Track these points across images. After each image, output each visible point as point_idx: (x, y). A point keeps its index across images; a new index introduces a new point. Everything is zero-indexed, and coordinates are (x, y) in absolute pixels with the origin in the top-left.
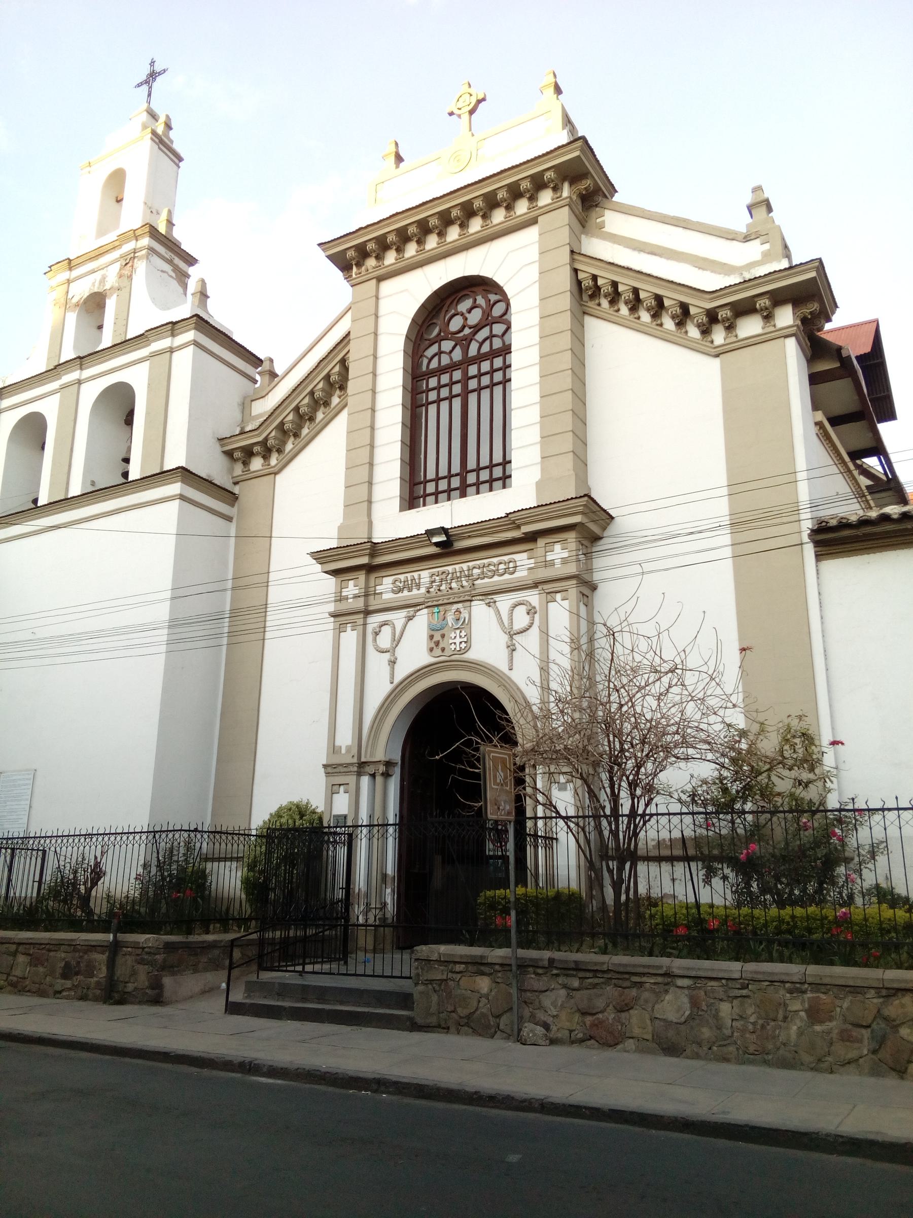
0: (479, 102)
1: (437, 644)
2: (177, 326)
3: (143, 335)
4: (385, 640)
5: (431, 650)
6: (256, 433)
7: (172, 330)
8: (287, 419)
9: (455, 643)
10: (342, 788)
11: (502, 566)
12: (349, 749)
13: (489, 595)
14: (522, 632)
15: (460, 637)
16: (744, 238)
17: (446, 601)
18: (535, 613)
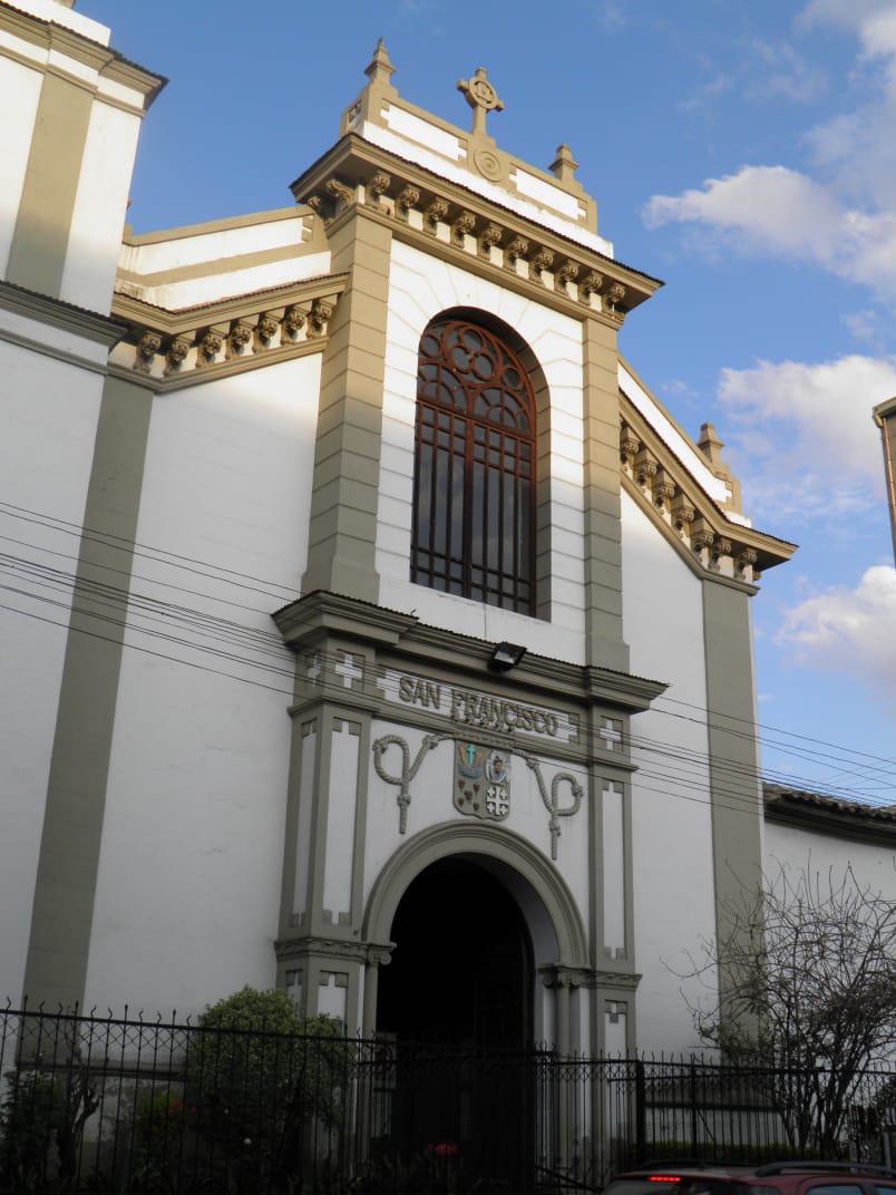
0: (498, 109)
1: (468, 796)
2: (116, 64)
3: (45, 23)
4: (392, 762)
5: (461, 802)
6: (171, 318)
7: (107, 64)
8: (218, 328)
9: (494, 804)
10: (332, 979)
11: (541, 725)
12: (346, 919)
13: (532, 752)
14: (567, 815)
15: (501, 797)
16: (717, 473)
17: (481, 741)
18: (582, 795)
